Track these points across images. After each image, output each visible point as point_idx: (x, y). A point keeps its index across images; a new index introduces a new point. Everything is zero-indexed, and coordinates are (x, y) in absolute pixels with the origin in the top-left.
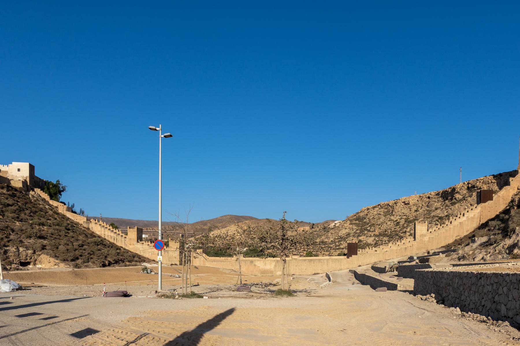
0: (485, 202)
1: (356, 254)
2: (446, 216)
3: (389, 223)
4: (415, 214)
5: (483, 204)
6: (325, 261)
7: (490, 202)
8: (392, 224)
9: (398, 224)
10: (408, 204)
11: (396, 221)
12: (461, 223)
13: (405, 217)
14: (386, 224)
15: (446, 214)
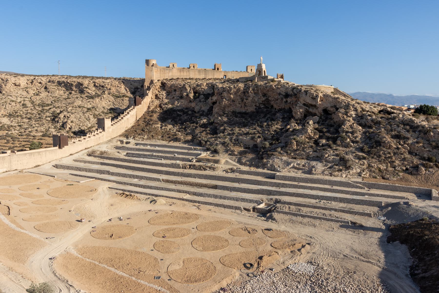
0: (138, 105)
1: (68, 145)
2: (93, 108)
3: (13, 104)
4: (38, 97)
5: (137, 107)
6: (44, 153)
7: (140, 105)
8: (18, 105)
9: (24, 105)
10: (19, 85)
11: (20, 102)
12: (128, 119)
13: (27, 99)
14: (10, 104)
15: (91, 106)
